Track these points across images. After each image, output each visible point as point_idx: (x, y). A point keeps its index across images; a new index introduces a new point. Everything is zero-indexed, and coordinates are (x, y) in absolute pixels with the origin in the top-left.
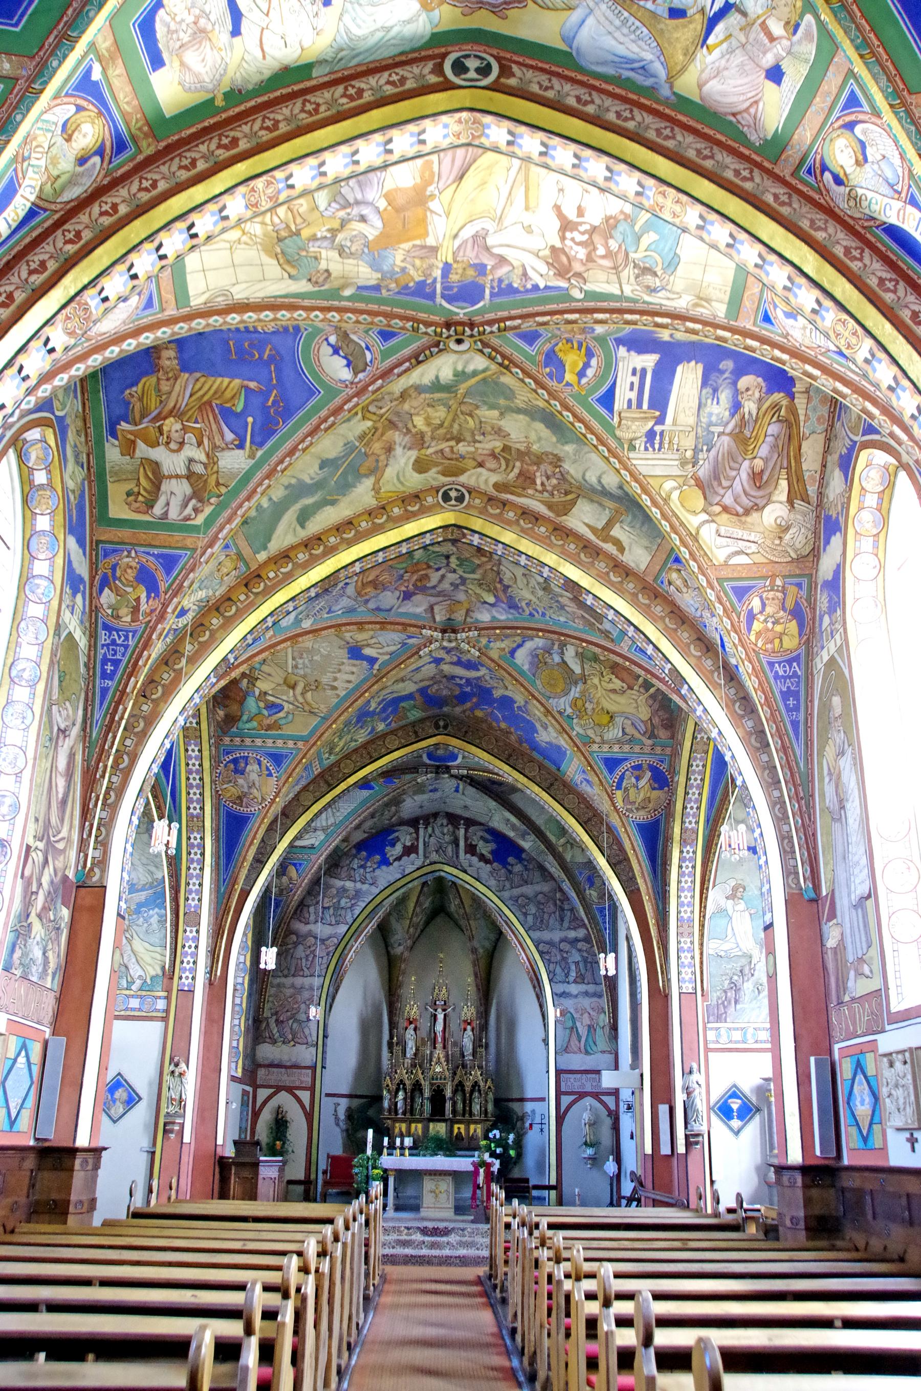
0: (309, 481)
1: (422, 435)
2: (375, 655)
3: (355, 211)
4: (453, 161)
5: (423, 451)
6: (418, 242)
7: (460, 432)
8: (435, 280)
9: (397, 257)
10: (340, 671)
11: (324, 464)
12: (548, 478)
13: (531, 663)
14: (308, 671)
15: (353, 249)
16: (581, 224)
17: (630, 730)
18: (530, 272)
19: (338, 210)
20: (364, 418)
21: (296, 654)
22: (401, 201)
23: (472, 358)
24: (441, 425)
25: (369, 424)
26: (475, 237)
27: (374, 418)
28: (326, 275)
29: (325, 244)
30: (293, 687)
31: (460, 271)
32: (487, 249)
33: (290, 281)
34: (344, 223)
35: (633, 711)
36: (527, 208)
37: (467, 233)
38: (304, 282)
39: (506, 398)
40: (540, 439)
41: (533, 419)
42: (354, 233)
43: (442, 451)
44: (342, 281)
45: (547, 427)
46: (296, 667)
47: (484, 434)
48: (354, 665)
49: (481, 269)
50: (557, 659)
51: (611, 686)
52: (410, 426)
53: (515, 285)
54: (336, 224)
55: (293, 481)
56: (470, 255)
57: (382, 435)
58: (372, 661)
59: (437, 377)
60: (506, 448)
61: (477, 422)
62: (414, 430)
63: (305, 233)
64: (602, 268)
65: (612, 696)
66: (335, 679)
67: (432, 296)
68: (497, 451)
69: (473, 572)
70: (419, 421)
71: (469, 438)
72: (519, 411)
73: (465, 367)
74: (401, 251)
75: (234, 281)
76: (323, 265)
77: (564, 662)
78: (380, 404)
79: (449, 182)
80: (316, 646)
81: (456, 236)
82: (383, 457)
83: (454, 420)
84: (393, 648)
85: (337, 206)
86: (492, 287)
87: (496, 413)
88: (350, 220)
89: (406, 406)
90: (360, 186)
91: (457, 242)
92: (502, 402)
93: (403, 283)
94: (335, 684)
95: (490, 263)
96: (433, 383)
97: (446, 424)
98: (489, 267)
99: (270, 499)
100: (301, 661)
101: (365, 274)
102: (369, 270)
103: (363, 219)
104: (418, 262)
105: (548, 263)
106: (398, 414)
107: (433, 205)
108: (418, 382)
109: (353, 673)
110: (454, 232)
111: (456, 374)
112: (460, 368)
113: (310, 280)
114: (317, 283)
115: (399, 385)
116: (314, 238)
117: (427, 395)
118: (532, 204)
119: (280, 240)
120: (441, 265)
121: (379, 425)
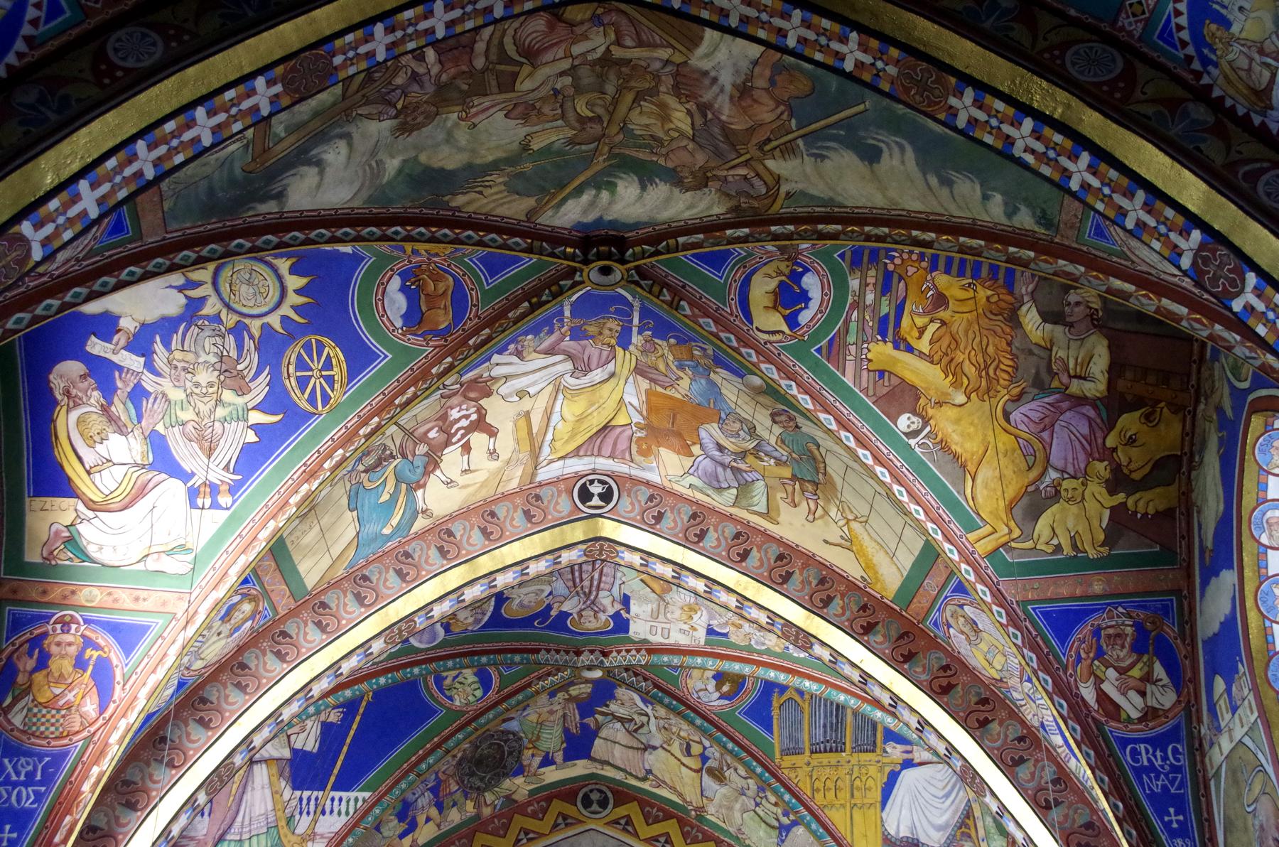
0: (910, 153)
1: (677, 91)
3: (727, 459)
4: (615, 444)
5: (678, 58)
6: (659, 389)
7: (602, 78)
8: (640, 333)
9: (685, 386)
11: (871, 155)
12: (415, 77)
15: (738, 425)
16: (463, 436)
18: (515, 359)
19: (745, 472)
20: (778, 180)
22: (675, 441)
23: (585, 212)
24: (639, 97)
25: (770, 164)
26: (588, 370)
27: (760, 169)
28: (777, 419)
29: (769, 449)
31: (606, 332)
32: (570, 357)
33: (820, 441)
34: (743, 455)
36: (527, 414)
37: (597, 375)
38: (804, 429)
39: (520, 175)
40: (450, 138)
41: (469, 167)
42: (733, 440)
43: (641, 44)
44: (761, 399)
45: (442, 170)
47: (556, 92)
49: (577, 334)
52: (699, 121)
53: (530, 337)
54: (750, 459)
55: (934, 181)
56: (592, 350)
57: (751, 131)
59: (643, 188)
60: (508, 84)
61: (571, 115)
62: (691, 106)
63: (786, 472)
64: (426, 421)
67: (645, 313)
68: (526, 69)
70: (681, 119)
71: (584, 72)
72: (495, 166)
73: (596, 196)
74: (683, 392)
75: (877, 496)
76: (777, 430)
78: (746, 188)
79: (619, 430)
81: (612, 375)
82: (761, 83)
83: (615, 102)
85: (745, 475)
86: (561, 321)
87: (536, 145)
88: (736, 454)
89: (701, 159)
90: (717, 477)
91: (611, 367)
92: (528, 167)
93: (683, 347)
95: (567, 344)
96: (652, 182)
97: (629, 97)
98: (568, 338)
99: (986, 197)
101: (730, 389)
102: (724, 391)
103: (721, 448)
104: (662, 367)
105: (493, 378)
106: (718, 153)
107: (637, 418)
108: (676, 191)
110: (613, 382)
111: (611, 187)
112: (605, 195)
113: (797, 427)
114: (790, 418)
115: (708, 205)
116: (779, 462)
117: (661, 161)
118: (522, 423)
119: (816, 484)
120: (631, 348)
121: (754, 152)
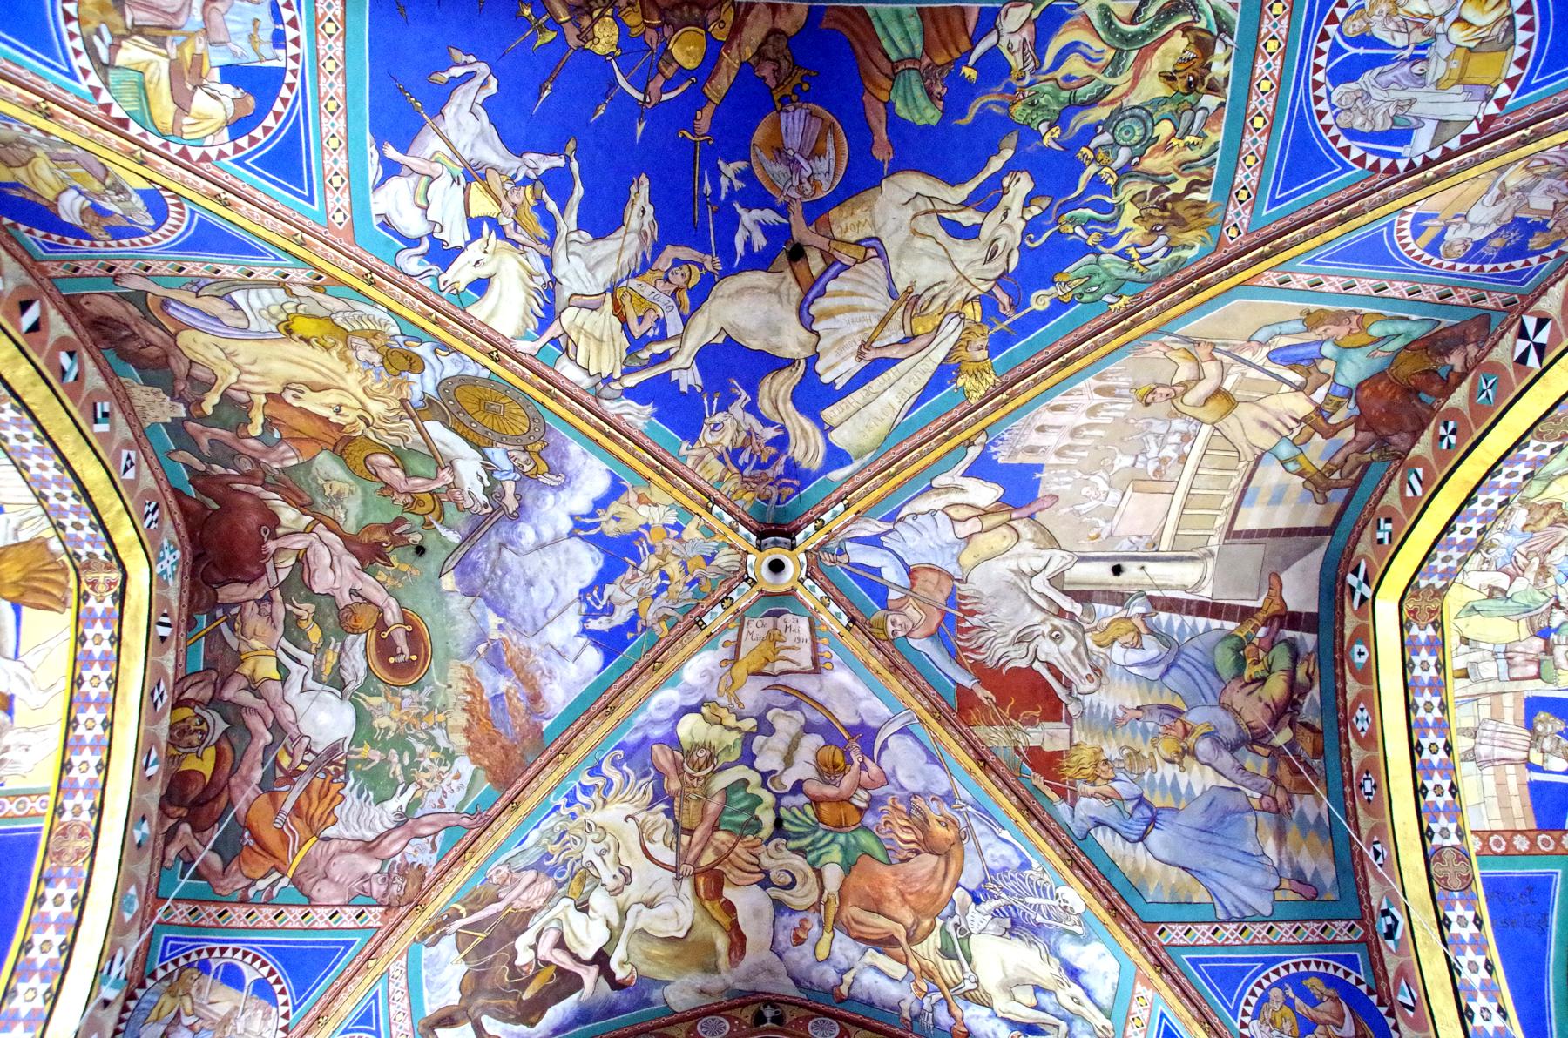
2: (970, 484)
10: (1075, 432)
13: (565, 456)
14: (1160, 427)
17: (220, 308)
21: (1171, 473)
30: (1218, 392)
35: (232, 346)
46: (1186, 437)
48: (1033, 450)
50: (498, 455)
51: (332, 397)
58: (983, 469)
65: (316, 377)
66: (1093, 411)
69: (728, 791)
77: (477, 447)
80: (1115, 496)
84: (921, 505)
94: (1098, 399)
100: (1169, 452)
109: (1041, 429)
